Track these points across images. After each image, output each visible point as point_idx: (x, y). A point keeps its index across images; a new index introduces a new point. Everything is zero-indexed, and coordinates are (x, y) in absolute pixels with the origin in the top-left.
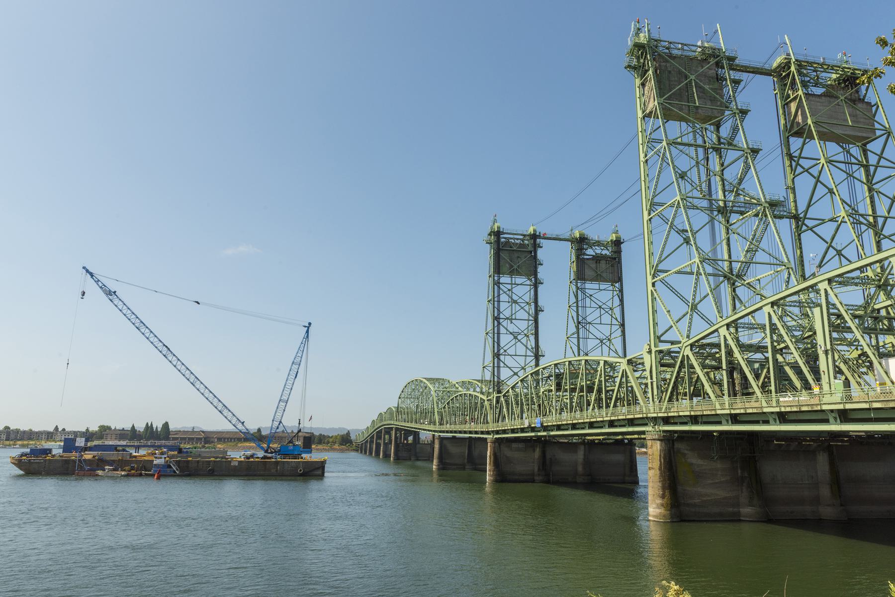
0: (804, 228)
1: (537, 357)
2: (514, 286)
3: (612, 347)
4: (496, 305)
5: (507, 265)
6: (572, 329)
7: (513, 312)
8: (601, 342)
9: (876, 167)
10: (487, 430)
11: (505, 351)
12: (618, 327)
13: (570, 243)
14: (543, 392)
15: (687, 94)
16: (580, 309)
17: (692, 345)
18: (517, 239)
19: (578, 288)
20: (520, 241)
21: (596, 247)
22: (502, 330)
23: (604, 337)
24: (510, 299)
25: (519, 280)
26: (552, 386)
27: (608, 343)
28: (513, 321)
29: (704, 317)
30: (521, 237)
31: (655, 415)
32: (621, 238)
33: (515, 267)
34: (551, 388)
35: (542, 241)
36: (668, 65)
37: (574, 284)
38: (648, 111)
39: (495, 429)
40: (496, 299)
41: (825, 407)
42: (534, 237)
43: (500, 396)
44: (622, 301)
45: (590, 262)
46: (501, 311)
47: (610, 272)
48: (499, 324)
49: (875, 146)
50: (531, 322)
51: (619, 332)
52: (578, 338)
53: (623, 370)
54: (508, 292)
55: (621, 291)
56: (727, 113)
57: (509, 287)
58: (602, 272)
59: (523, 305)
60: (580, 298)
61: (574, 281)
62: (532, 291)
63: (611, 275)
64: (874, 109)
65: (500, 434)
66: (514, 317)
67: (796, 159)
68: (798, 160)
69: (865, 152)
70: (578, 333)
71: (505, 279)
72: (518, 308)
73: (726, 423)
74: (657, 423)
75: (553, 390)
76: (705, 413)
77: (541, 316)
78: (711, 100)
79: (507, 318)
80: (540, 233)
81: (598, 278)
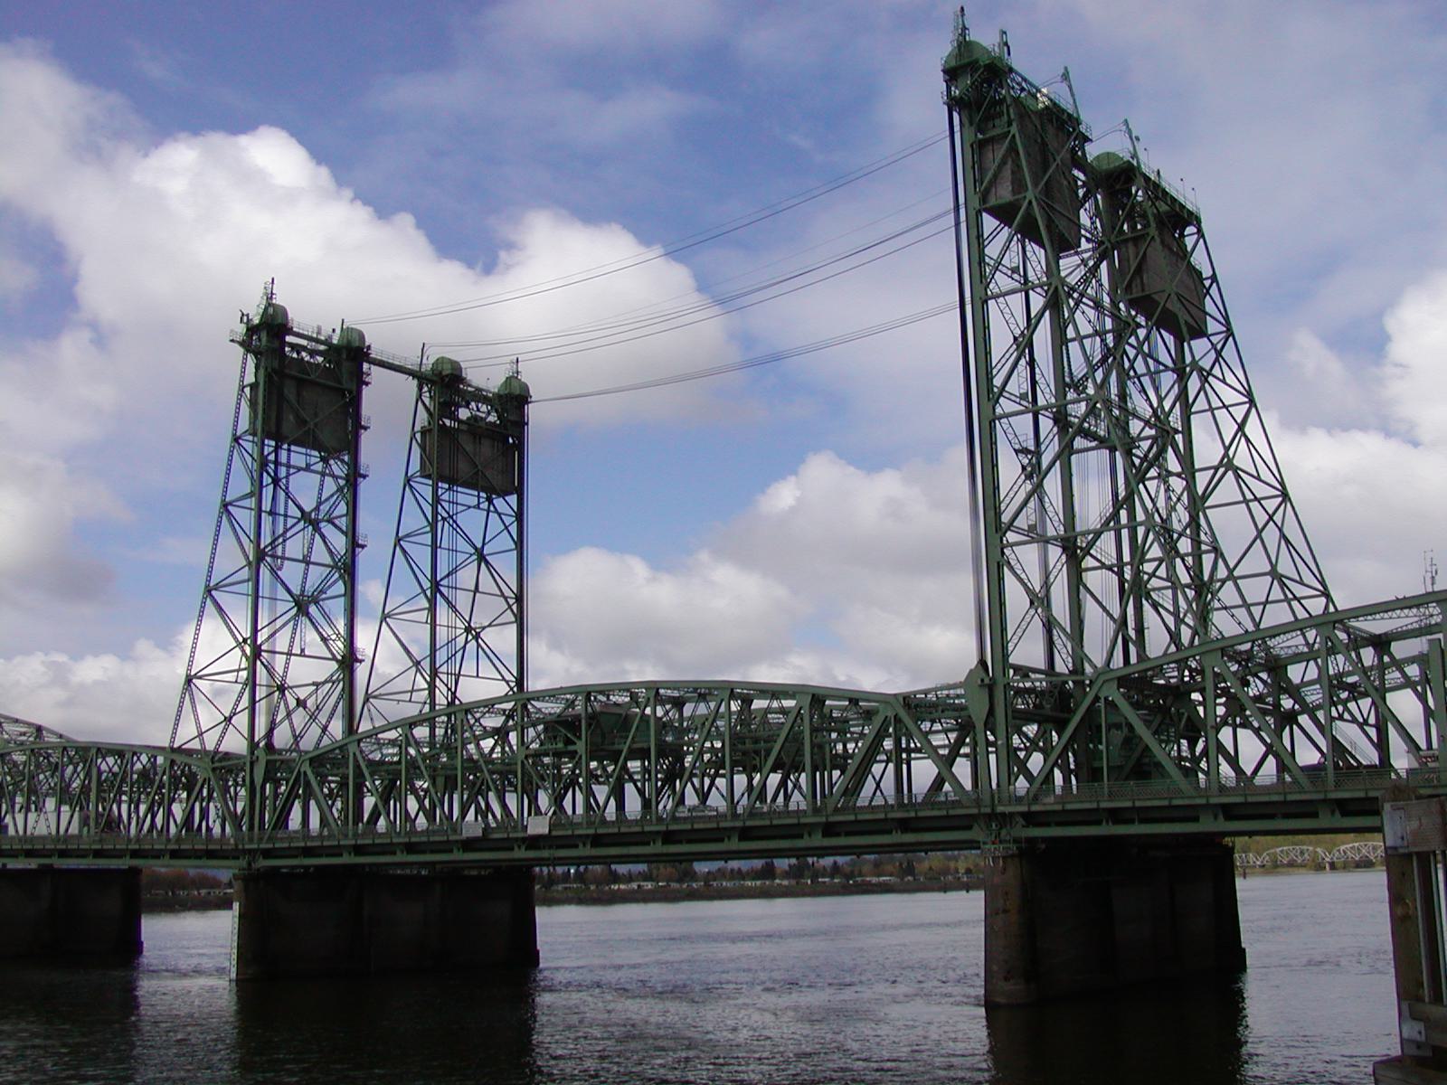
34: (571, 748)
44: (520, 544)
55: (520, 516)
63: (500, 477)
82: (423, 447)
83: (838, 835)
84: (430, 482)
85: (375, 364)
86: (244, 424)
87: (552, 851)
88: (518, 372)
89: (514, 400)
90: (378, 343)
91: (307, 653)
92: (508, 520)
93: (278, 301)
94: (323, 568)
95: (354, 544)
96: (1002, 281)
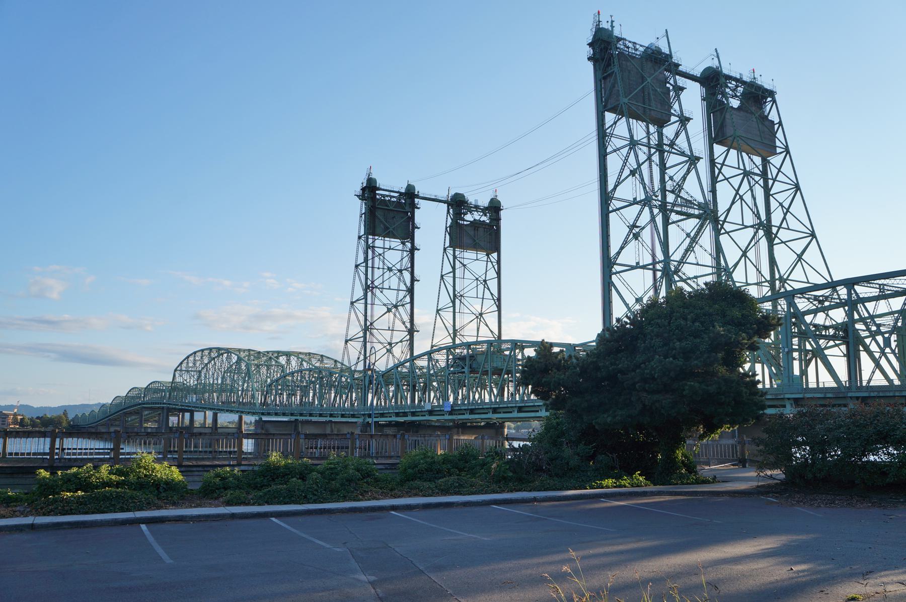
0: (723, 231)
5: (382, 226)
9: (775, 180)
13: (446, 205)
15: (642, 95)
18: (394, 197)
19: (455, 257)
22: (377, 301)
25: (395, 243)
26: (463, 368)
33: (391, 230)
34: (463, 370)
35: (421, 201)
36: (628, 64)
37: (452, 252)
38: (609, 106)
41: (787, 396)
42: (410, 195)
44: (499, 273)
47: (488, 241)
49: (776, 160)
51: (495, 308)
52: (454, 312)
55: (499, 262)
56: (673, 119)
57: (380, 251)
64: (776, 127)
66: (386, 285)
67: (719, 166)
68: (721, 167)
69: (765, 162)
71: (379, 242)
75: (466, 372)
78: (661, 104)
80: (418, 192)
81: (476, 247)
84: (452, 249)
86: (362, 233)
87: (456, 416)
89: (494, 208)
90: (420, 189)
93: (373, 176)
94: (403, 292)
95: (413, 280)
96: (615, 143)
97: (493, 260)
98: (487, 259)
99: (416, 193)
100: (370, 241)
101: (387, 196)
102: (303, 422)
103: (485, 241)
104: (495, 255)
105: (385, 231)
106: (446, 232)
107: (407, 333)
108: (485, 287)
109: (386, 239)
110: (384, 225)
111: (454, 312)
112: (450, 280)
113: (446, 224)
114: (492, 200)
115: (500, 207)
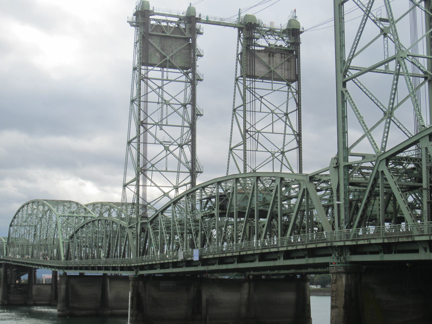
1: (193, 173)
2: (165, 82)
3: (285, 162)
4: (142, 107)
5: (158, 54)
6: (238, 138)
7: (164, 116)
8: (273, 155)
10: (128, 265)
11: (153, 166)
12: (293, 137)
13: (236, 30)
14: (202, 217)
16: (248, 114)
17: (387, 160)
18: (172, 22)
19: (245, 88)
20: (174, 24)
21: (269, 36)
22: (150, 139)
23: (277, 150)
24: (160, 99)
27: (280, 157)
28: (164, 127)
29: (401, 126)
30: (176, 19)
31: (342, 244)
32: (300, 26)
33: (168, 58)
34: (213, 212)
35: (203, 25)
37: (242, 82)
39: (140, 264)
40: (142, 99)
43: (146, 223)
44: (299, 105)
45: (263, 54)
46: (149, 115)
47: (286, 68)
48: (146, 130)
50: (186, 130)
51: (295, 144)
52: (245, 150)
53: (304, 189)
54: (158, 90)
55: (298, 92)
57: (159, 83)
58: (276, 68)
59: (176, 107)
60: (248, 101)
61: (242, 78)
62: (189, 90)
63: (286, 72)
65: (146, 270)
66: (164, 122)
70: (244, 143)
72: (170, 110)
73: (424, 252)
74: (343, 254)
75: (216, 214)
76: (400, 240)
77: (199, 122)
79: (156, 124)
80: (200, 15)
82: (241, 62)
83: (293, 258)
85: (203, 23)
88: (296, 17)
91: (168, 170)
92: (295, 94)
97: (294, 90)
98: (288, 89)
99: (197, 16)
100: (143, 72)
101: (164, 21)
102: (112, 278)
103: (282, 69)
104: (294, 85)
105: (161, 60)
106: (237, 60)
107: (189, 174)
108: (286, 124)
109: (165, 69)
110: (160, 53)
111: (245, 150)
112: (242, 113)
113: (238, 51)
114: (290, 21)
115: (299, 29)
